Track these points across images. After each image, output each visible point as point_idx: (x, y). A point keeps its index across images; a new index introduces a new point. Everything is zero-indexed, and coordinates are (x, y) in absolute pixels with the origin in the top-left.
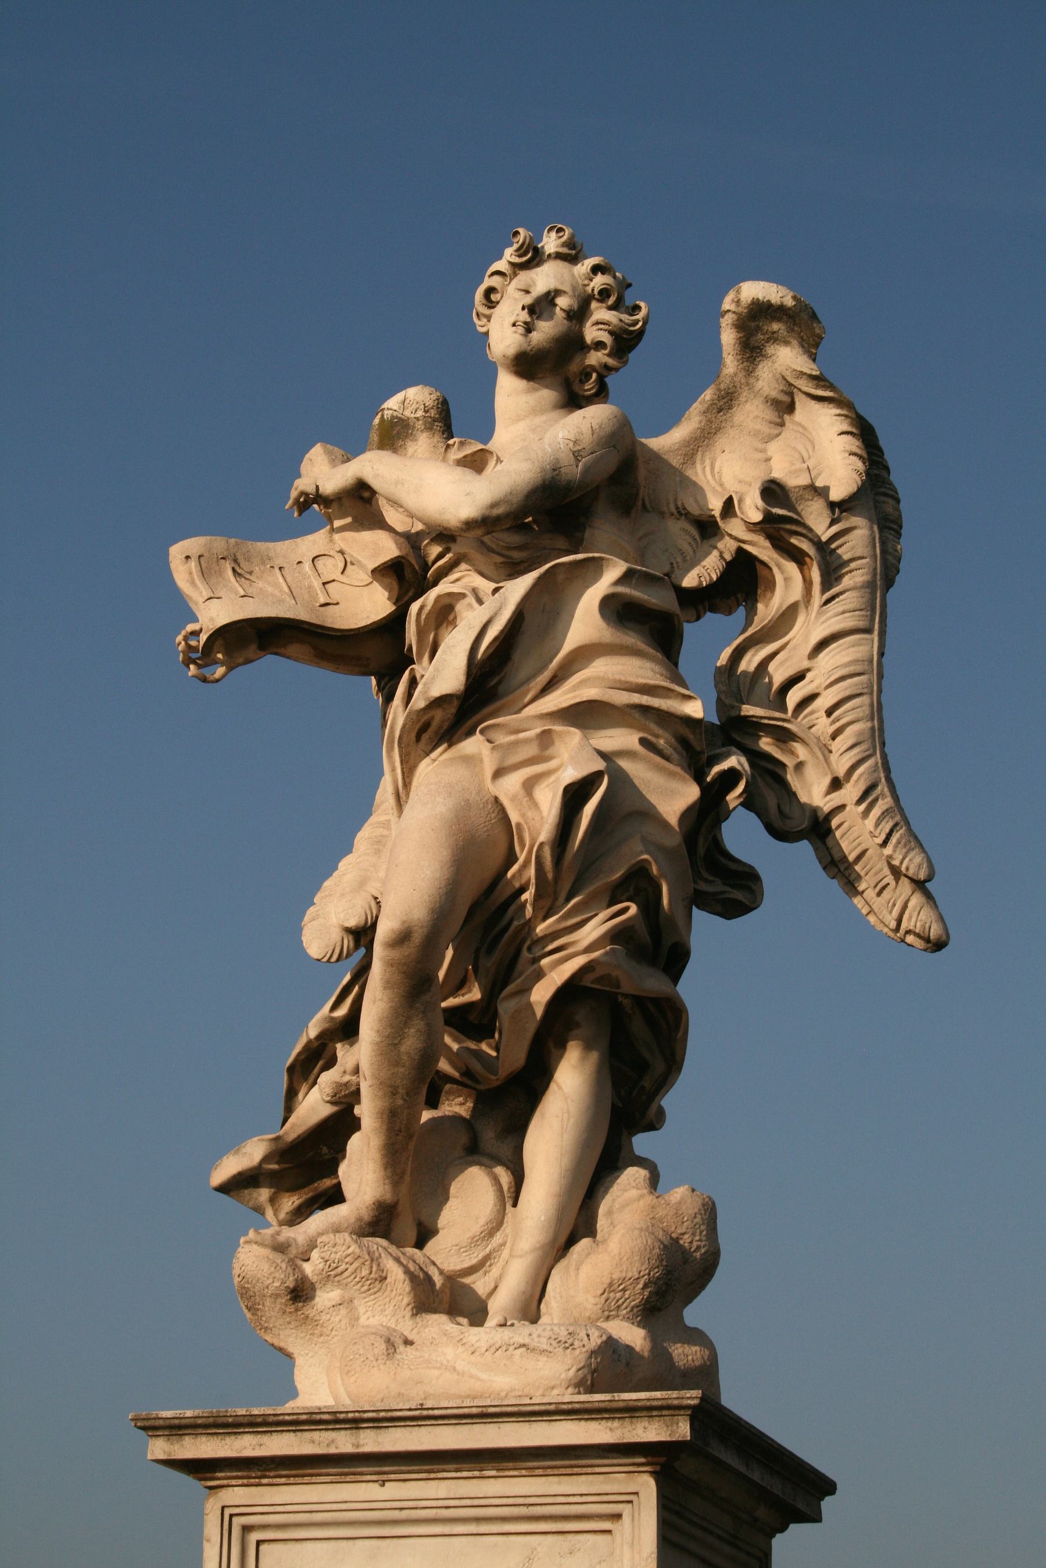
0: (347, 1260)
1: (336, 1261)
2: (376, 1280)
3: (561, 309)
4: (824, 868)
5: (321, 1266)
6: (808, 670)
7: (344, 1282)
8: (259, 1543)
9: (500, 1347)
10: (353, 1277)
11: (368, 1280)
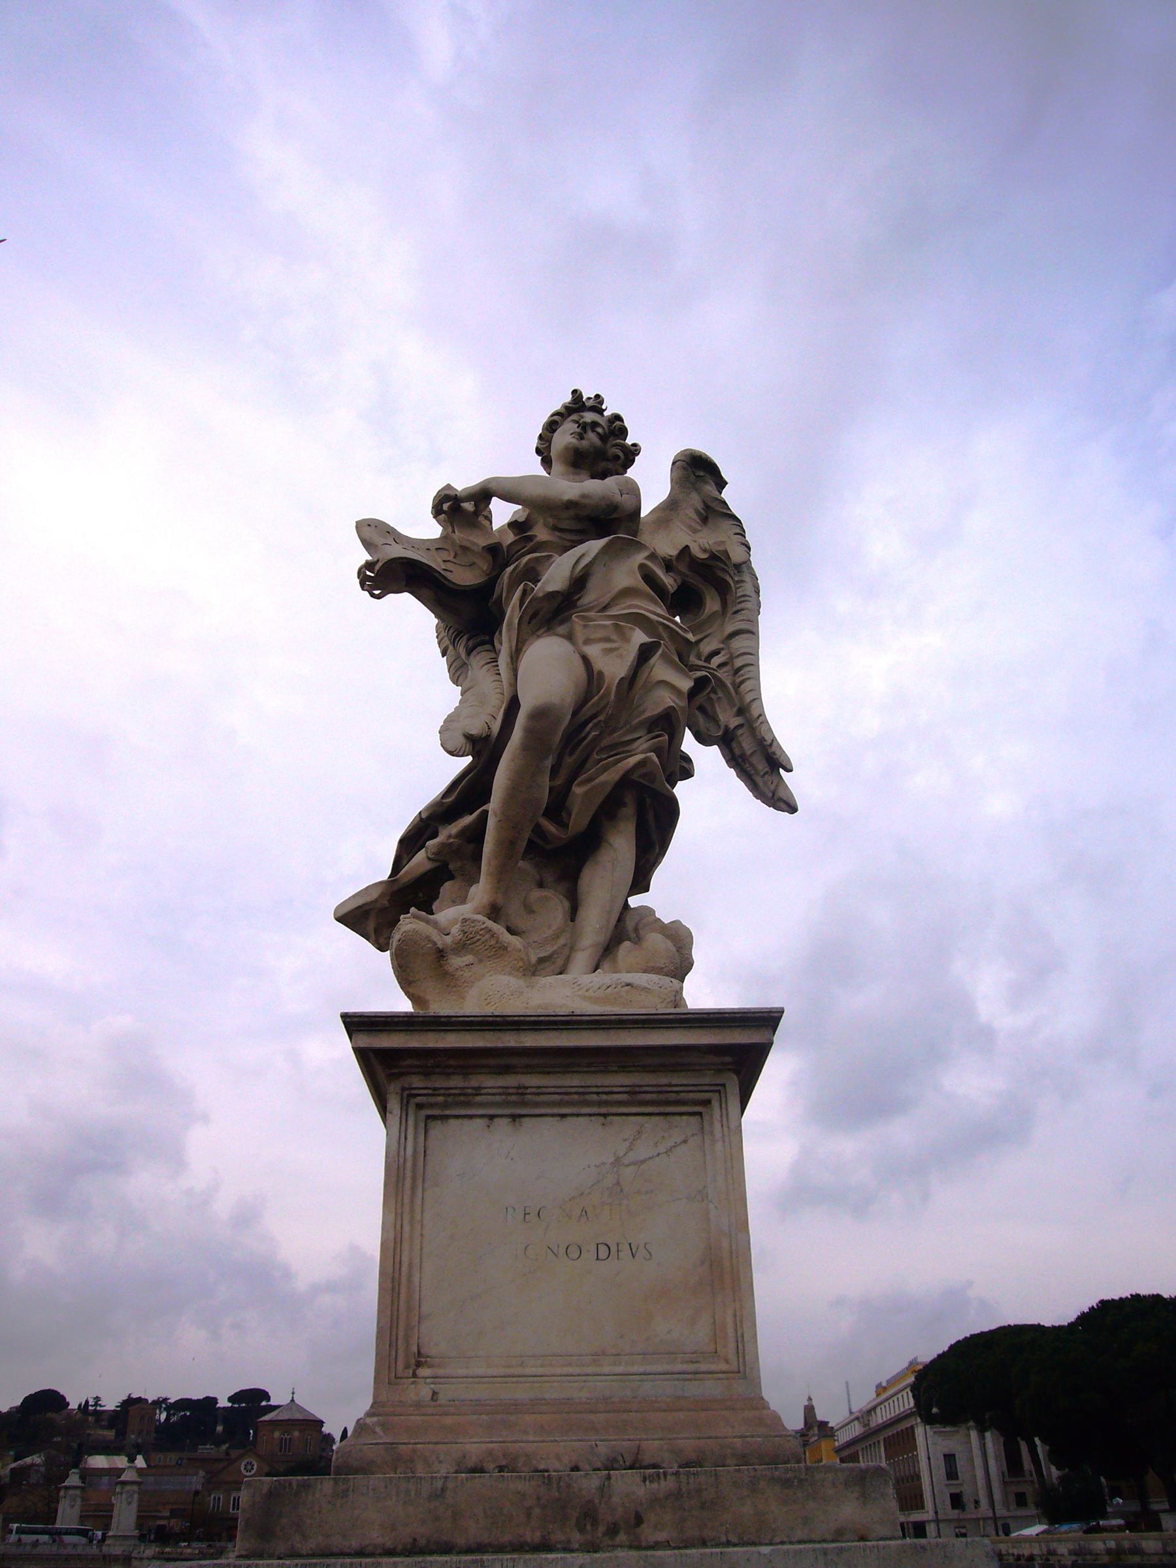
0: (481, 933)
1: (473, 933)
2: (500, 948)
3: (598, 434)
4: (727, 762)
5: (460, 937)
6: (723, 649)
7: (477, 949)
8: (428, 1117)
9: (610, 986)
10: (483, 945)
11: (494, 948)
